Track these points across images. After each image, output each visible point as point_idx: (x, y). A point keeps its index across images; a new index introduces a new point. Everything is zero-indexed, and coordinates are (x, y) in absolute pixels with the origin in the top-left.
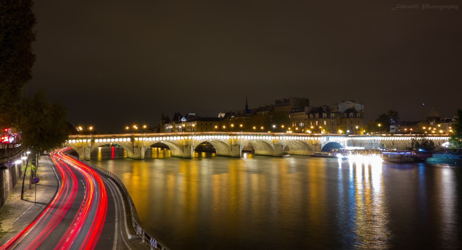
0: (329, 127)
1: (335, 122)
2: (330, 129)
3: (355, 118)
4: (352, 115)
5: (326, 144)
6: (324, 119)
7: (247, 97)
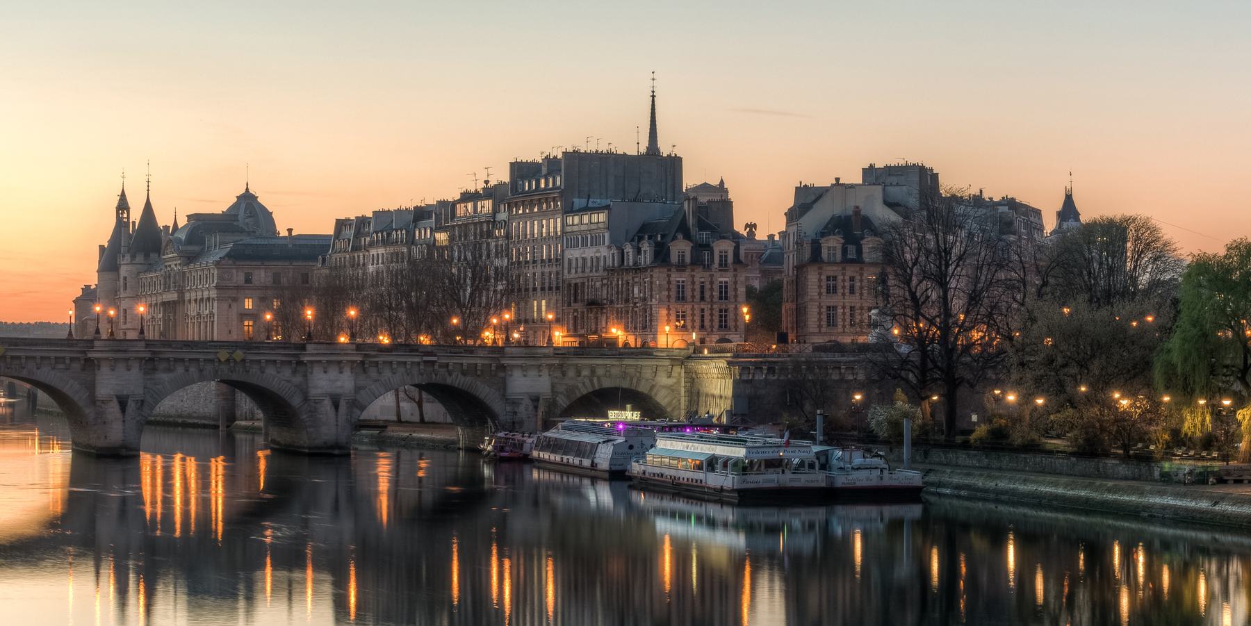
0: (703, 310)
1: (736, 283)
2: (707, 323)
3: (852, 261)
4: (835, 248)
5: (579, 395)
6: (673, 270)
7: (653, 97)
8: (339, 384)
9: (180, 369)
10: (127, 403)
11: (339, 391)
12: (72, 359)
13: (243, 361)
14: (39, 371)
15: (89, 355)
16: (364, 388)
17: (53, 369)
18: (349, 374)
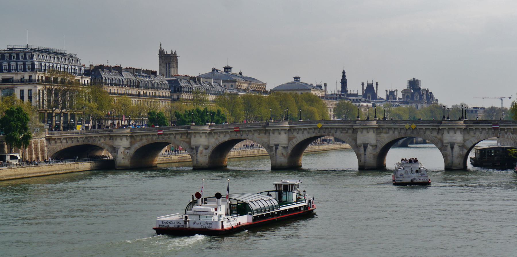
8: (454, 138)
9: (391, 132)
10: (367, 147)
11: (454, 141)
12: (348, 129)
13: (415, 128)
14: (336, 134)
15: (355, 127)
16: (468, 140)
17: (341, 133)
18: (460, 134)
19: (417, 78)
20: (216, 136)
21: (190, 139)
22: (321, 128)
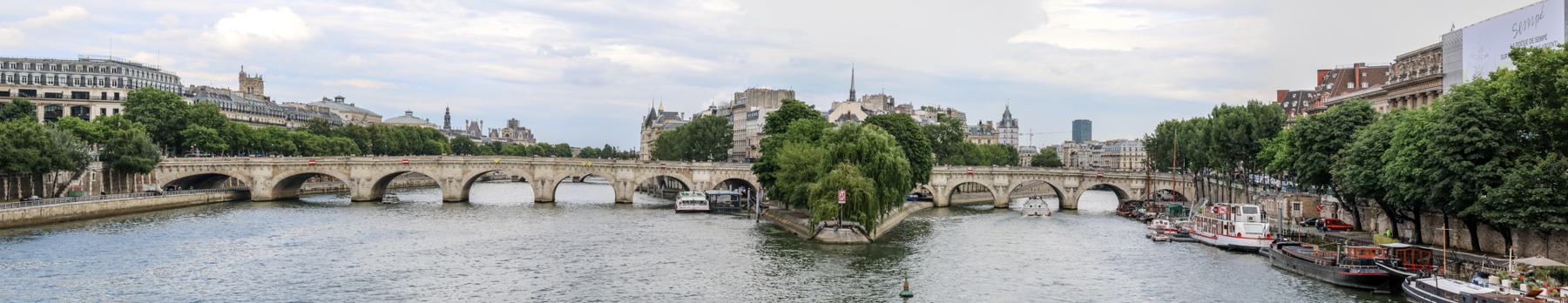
9: (568, 168)
19: (516, 119)
20: (380, 168)
21: (350, 169)
22: (498, 163)
